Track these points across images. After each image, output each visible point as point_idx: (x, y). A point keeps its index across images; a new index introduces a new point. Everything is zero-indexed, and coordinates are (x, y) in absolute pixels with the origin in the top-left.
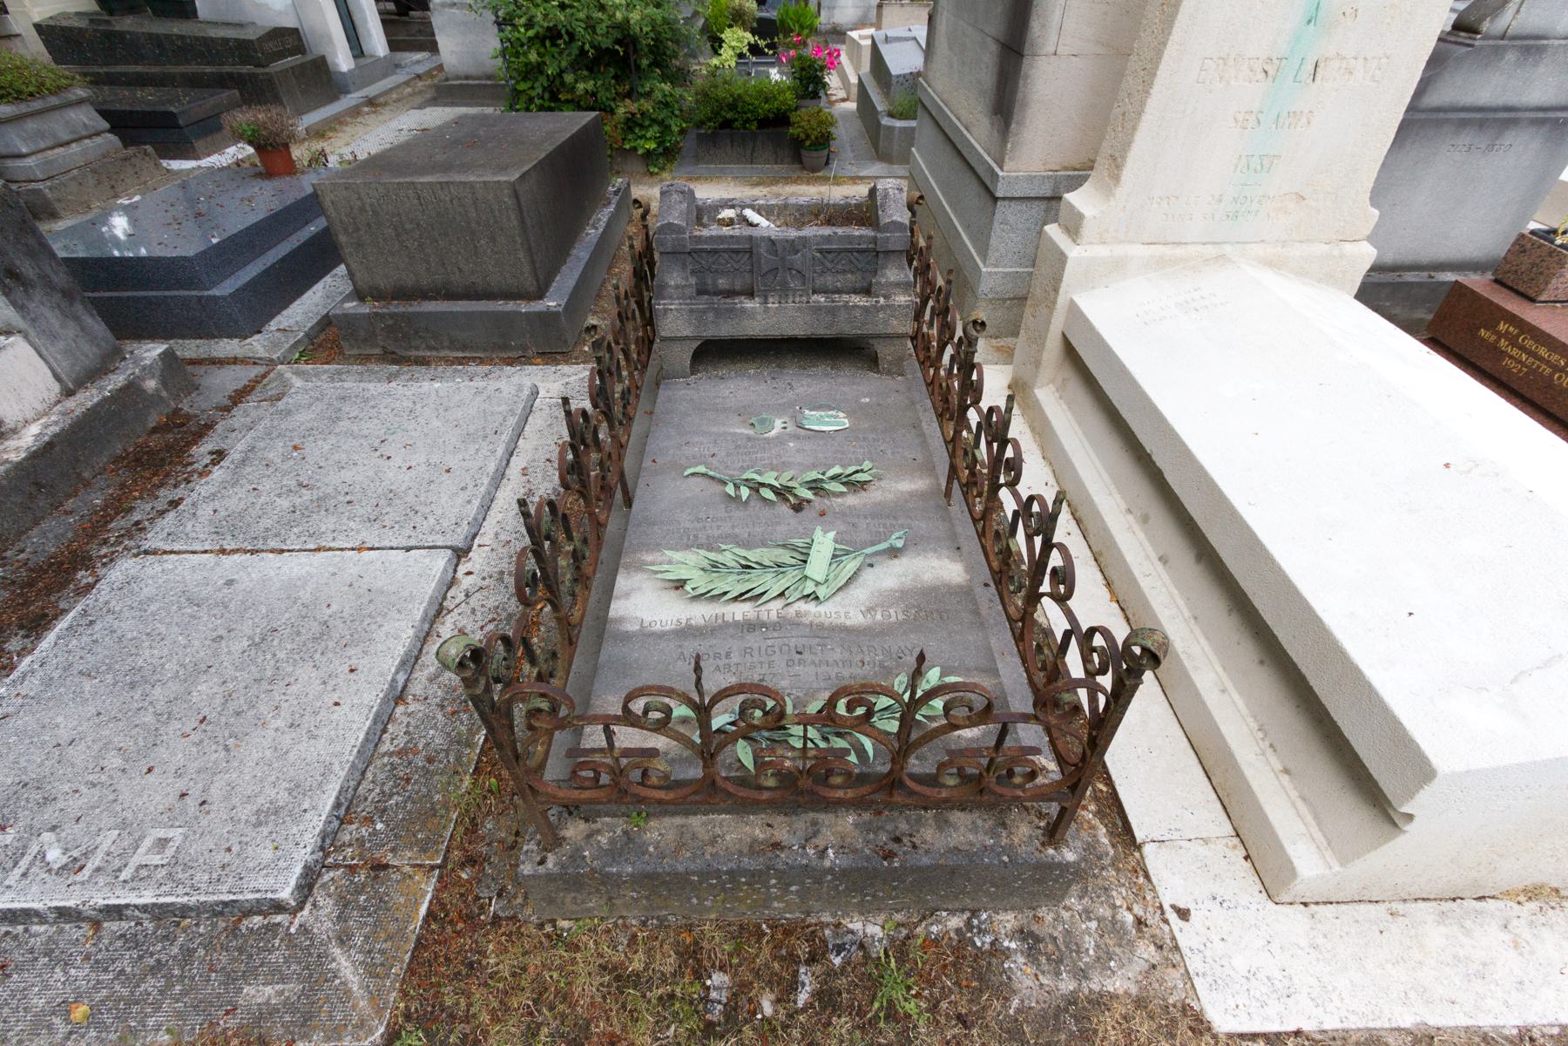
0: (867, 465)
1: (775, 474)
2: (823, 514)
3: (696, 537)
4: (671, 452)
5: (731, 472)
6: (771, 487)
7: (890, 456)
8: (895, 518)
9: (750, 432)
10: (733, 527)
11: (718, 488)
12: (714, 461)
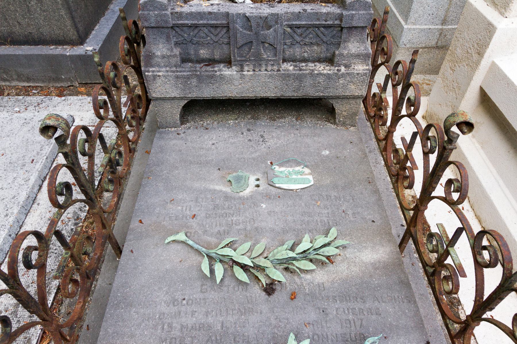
0: (333, 233)
1: (247, 246)
2: (293, 296)
3: (170, 326)
4: (157, 210)
5: (209, 239)
6: (244, 267)
7: (351, 215)
8: (363, 300)
9: (227, 189)
10: (207, 314)
11: (194, 258)
12: (193, 223)
